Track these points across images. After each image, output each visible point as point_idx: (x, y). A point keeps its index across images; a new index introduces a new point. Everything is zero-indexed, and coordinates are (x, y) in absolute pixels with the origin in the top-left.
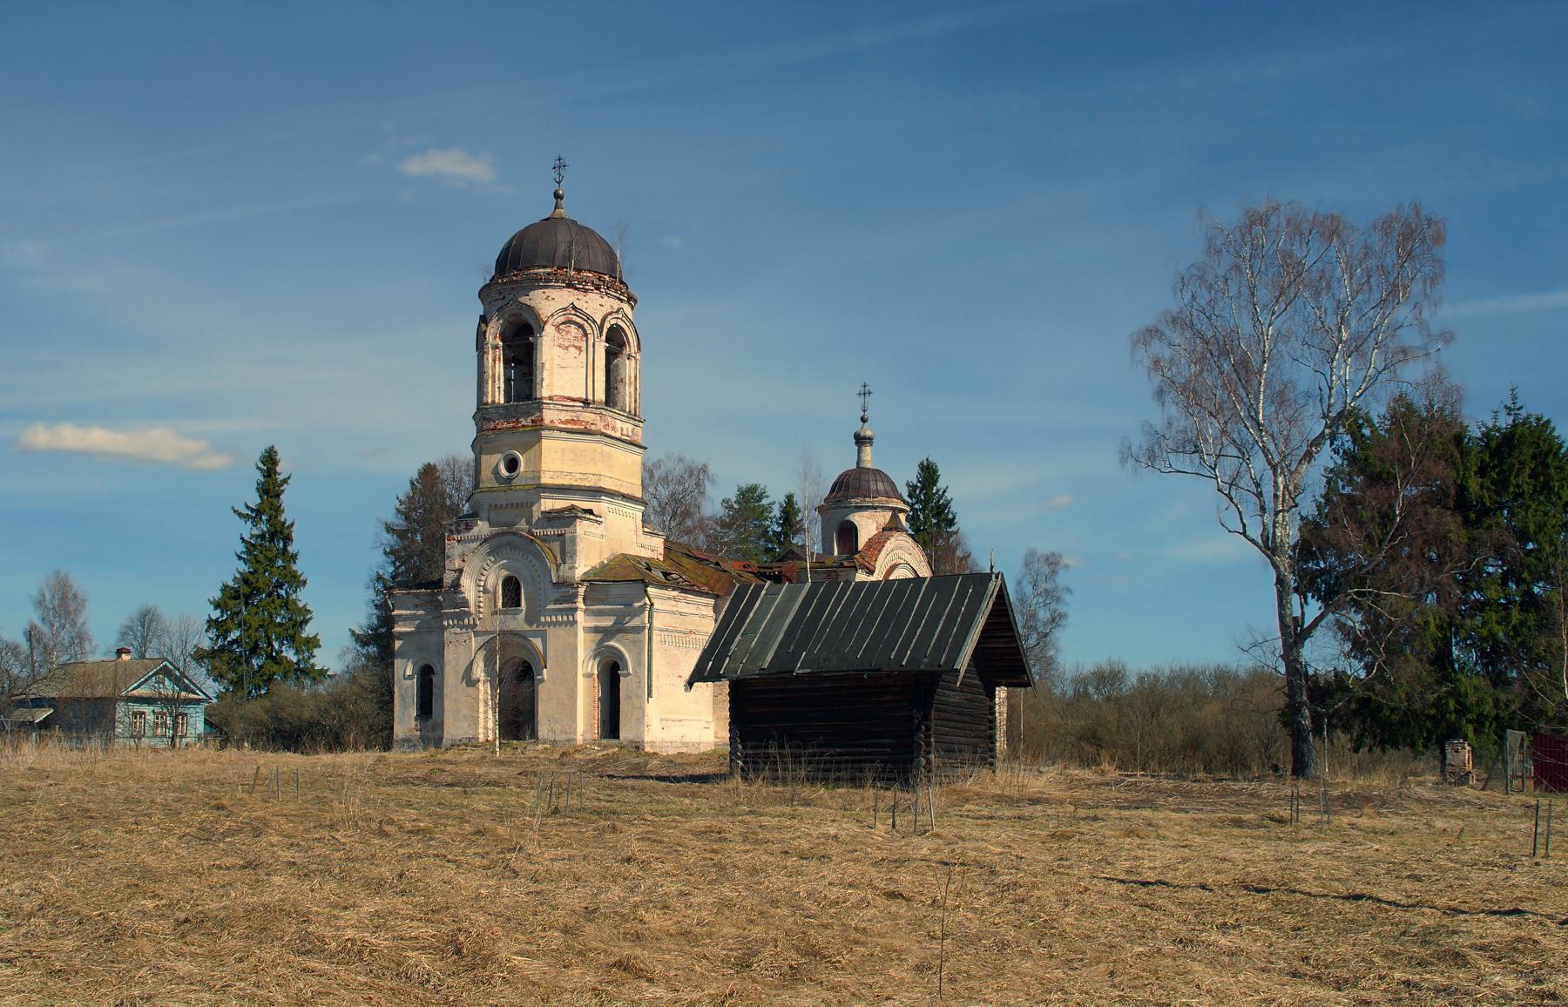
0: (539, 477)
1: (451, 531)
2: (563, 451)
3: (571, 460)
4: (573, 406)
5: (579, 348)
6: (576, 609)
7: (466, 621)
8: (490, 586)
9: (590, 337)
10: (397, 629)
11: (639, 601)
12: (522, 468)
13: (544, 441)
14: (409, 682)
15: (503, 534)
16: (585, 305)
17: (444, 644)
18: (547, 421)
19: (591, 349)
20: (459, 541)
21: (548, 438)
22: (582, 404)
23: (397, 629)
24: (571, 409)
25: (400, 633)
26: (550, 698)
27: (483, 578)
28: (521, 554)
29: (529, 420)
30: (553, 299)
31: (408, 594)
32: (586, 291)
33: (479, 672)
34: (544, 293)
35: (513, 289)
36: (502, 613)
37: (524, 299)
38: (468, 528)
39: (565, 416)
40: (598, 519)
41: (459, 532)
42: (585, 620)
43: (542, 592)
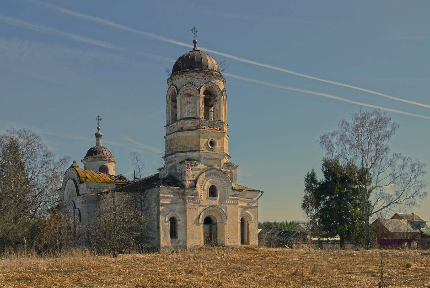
1: (188, 165)
7: (196, 201)
8: (206, 188)
11: (255, 198)
14: (167, 224)
17: (186, 209)
20: (191, 170)
23: (161, 202)
25: (163, 204)
26: (229, 231)
28: (218, 177)
29: (218, 128)
31: (168, 188)
35: (210, 77)
38: (196, 165)
41: (192, 166)
43: (226, 192)
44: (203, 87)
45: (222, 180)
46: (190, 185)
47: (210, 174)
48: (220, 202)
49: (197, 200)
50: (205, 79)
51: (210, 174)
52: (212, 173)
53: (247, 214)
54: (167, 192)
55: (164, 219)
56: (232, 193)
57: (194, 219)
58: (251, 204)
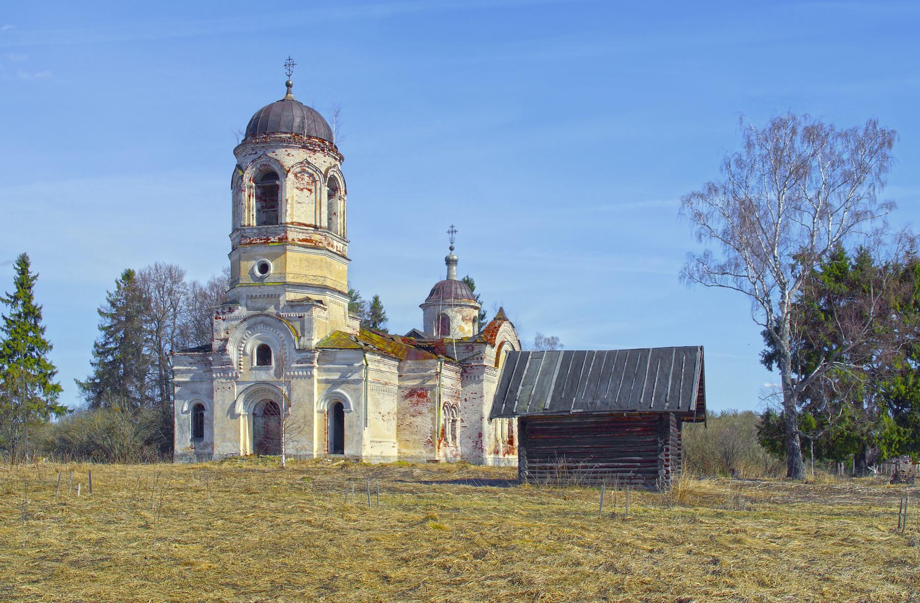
0: (285, 278)
1: (218, 313)
2: (301, 259)
3: (306, 266)
4: (307, 230)
5: (310, 190)
6: (313, 367)
7: (230, 375)
8: (248, 350)
9: (318, 183)
10: (176, 379)
11: (358, 362)
12: (272, 270)
13: (289, 254)
14: (186, 416)
15: (258, 315)
16: (314, 161)
18: (290, 239)
19: (318, 191)
20: (224, 320)
21: (291, 251)
22: (313, 229)
24: (306, 231)
25: (179, 382)
27: (243, 345)
28: (272, 329)
30: (293, 155)
31: (185, 355)
32: (315, 151)
33: (240, 408)
34: (286, 151)
35: (263, 147)
36: (255, 369)
37: (271, 155)
39: (301, 236)
40: (325, 307)
41: (224, 313)
42: (319, 375)
44: (250, 168)
45: (278, 333)
46: (220, 347)
47: (255, 324)
48: (278, 374)
49: (232, 373)
50: (256, 153)
51: (255, 324)
52: (261, 323)
53: (340, 396)
54: (186, 363)
55: (180, 409)
56: (298, 357)
57: (227, 409)
58: (350, 374)
